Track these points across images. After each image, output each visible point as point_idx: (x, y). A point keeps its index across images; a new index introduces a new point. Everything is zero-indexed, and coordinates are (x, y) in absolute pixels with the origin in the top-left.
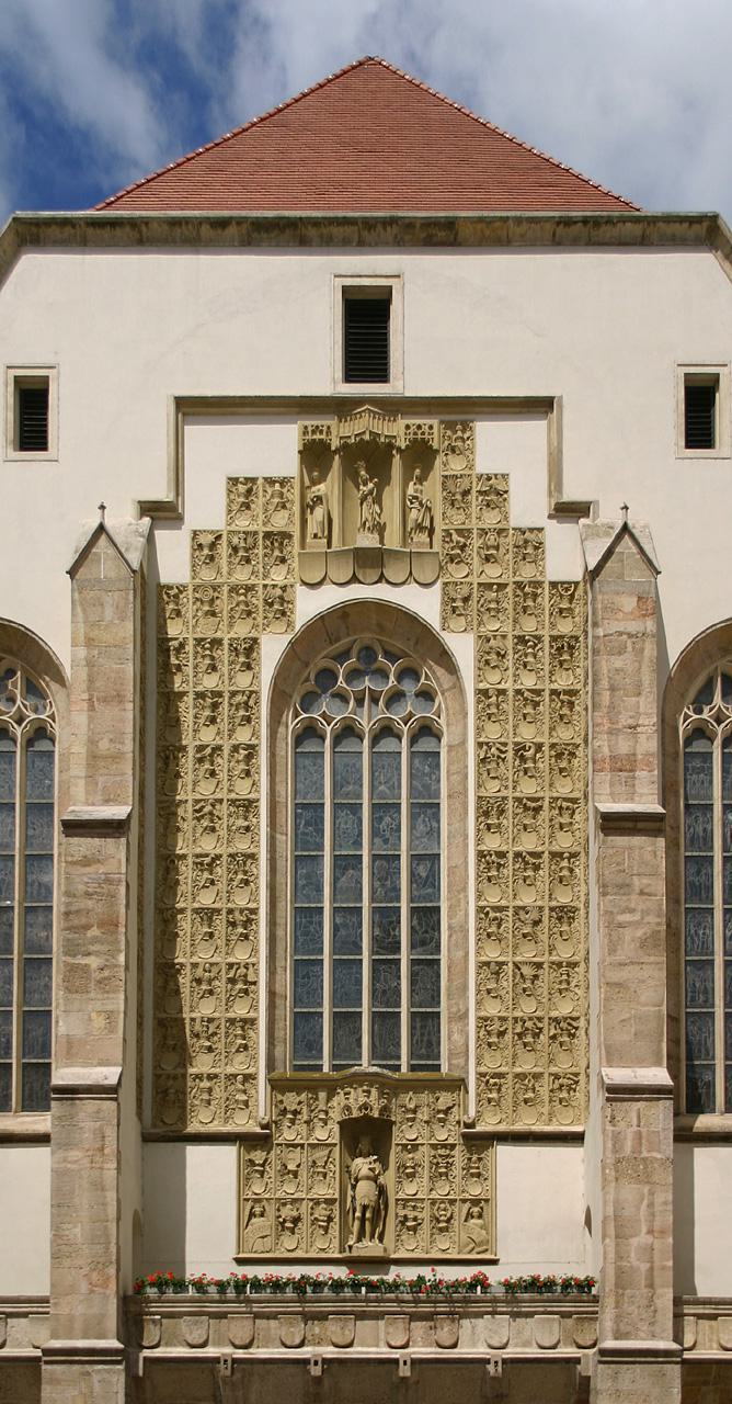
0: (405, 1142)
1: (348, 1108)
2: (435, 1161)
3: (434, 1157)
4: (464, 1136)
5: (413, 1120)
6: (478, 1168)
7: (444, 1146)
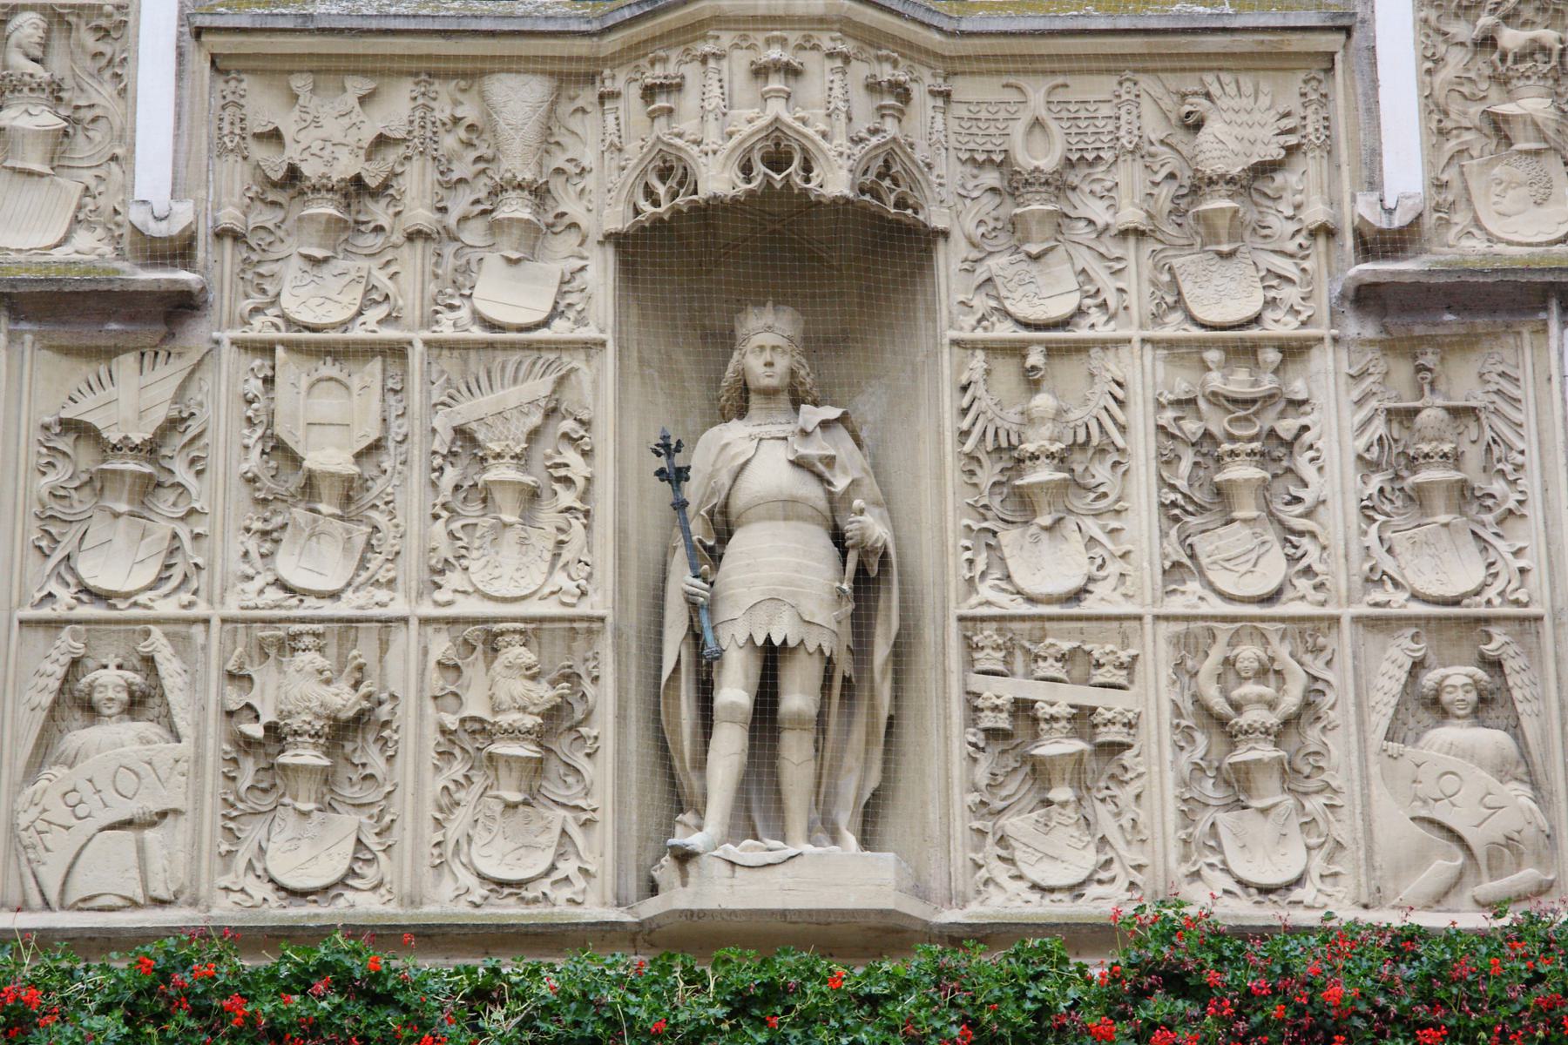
0: (1005, 331)
1: (671, 168)
2: (1192, 427)
3: (1186, 403)
4: (1366, 298)
5: (1061, 221)
6: (1454, 459)
7: (1245, 352)
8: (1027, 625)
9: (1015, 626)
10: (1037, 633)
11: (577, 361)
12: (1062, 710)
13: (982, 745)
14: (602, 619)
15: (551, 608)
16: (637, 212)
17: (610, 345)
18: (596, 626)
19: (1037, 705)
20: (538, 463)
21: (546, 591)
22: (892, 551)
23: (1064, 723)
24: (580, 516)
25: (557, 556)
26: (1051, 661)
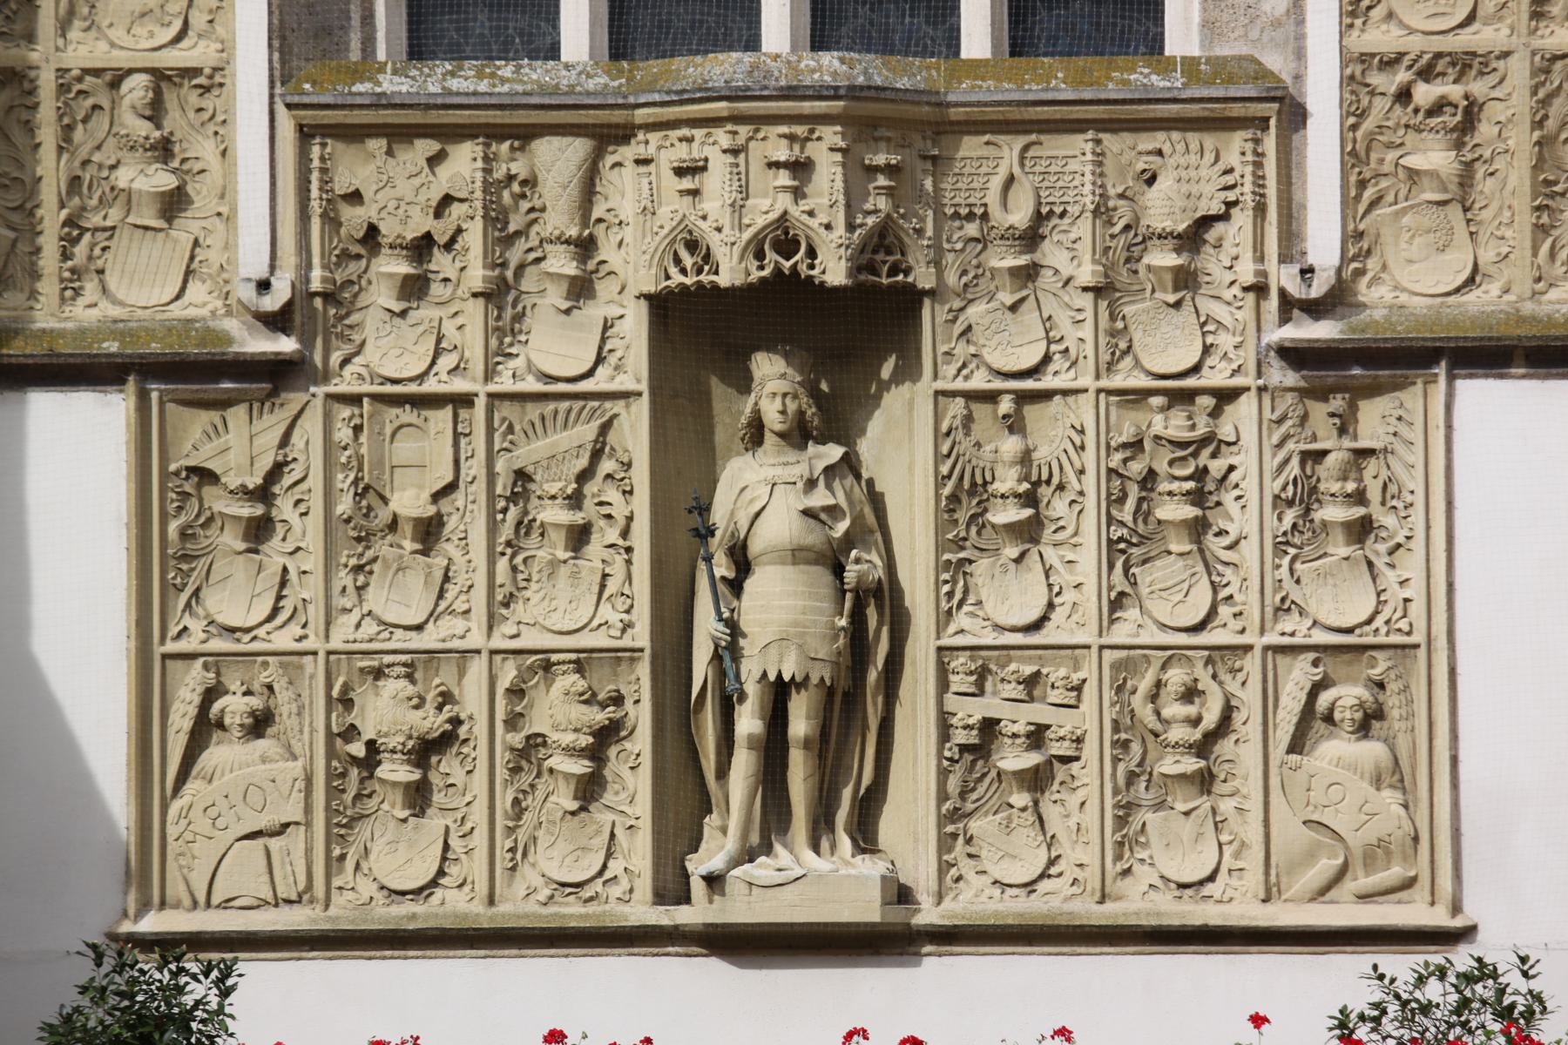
8: (996, 653)
9: (984, 653)
10: (1003, 660)
11: (618, 407)
12: (1020, 728)
13: (957, 757)
14: (641, 650)
15: (599, 640)
16: (668, 277)
17: (646, 396)
18: (636, 655)
19: (1002, 724)
20: (588, 503)
21: (595, 623)
22: (886, 586)
23: (1023, 739)
24: (622, 551)
25: (603, 587)
26: (1014, 685)
